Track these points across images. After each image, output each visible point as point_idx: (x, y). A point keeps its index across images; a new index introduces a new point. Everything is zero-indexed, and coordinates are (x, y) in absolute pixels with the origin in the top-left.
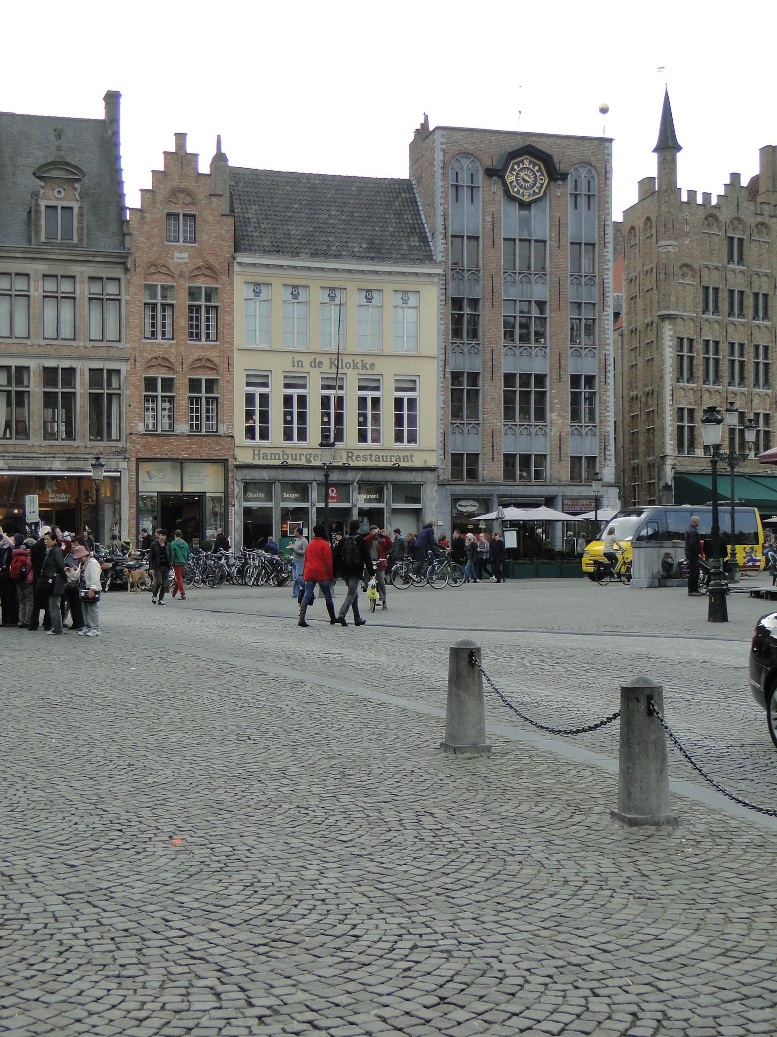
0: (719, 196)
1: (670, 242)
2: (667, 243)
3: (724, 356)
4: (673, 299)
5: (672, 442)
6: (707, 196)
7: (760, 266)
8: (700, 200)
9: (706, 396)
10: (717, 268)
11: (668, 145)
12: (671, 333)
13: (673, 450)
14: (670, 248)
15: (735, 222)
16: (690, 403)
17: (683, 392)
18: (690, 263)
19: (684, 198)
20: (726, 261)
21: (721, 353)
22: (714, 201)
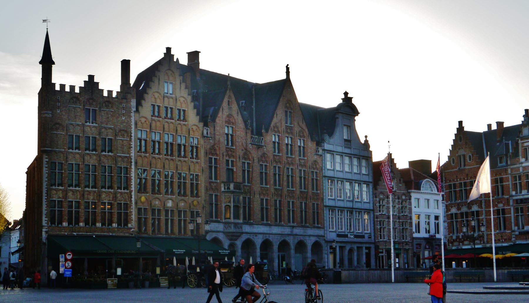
0: (80, 88)
1: (46, 112)
2: (45, 112)
3: (82, 172)
4: (48, 142)
5: (47, 219)
6: (72, 88)
7: (107, 124)
8: (67, 89)
9: (70, 194)
10: (78, 125)
11: (47, 62)
12: (47, 160)
13: (48, 223)
14: (46, 115)
15: (91, 101)
16: (59, 198)
17: (55, 192)
18: (60, 122)
19: (57, 88)
20: (84, 122)
21: (80, 170)
22: (77, 90)
